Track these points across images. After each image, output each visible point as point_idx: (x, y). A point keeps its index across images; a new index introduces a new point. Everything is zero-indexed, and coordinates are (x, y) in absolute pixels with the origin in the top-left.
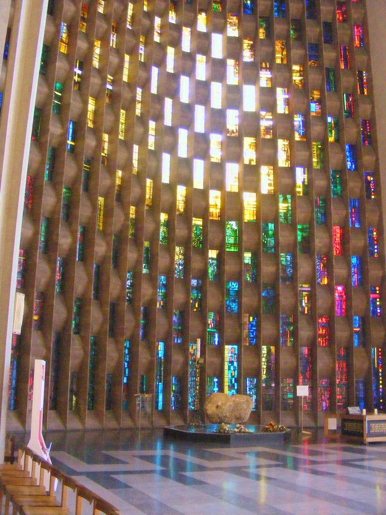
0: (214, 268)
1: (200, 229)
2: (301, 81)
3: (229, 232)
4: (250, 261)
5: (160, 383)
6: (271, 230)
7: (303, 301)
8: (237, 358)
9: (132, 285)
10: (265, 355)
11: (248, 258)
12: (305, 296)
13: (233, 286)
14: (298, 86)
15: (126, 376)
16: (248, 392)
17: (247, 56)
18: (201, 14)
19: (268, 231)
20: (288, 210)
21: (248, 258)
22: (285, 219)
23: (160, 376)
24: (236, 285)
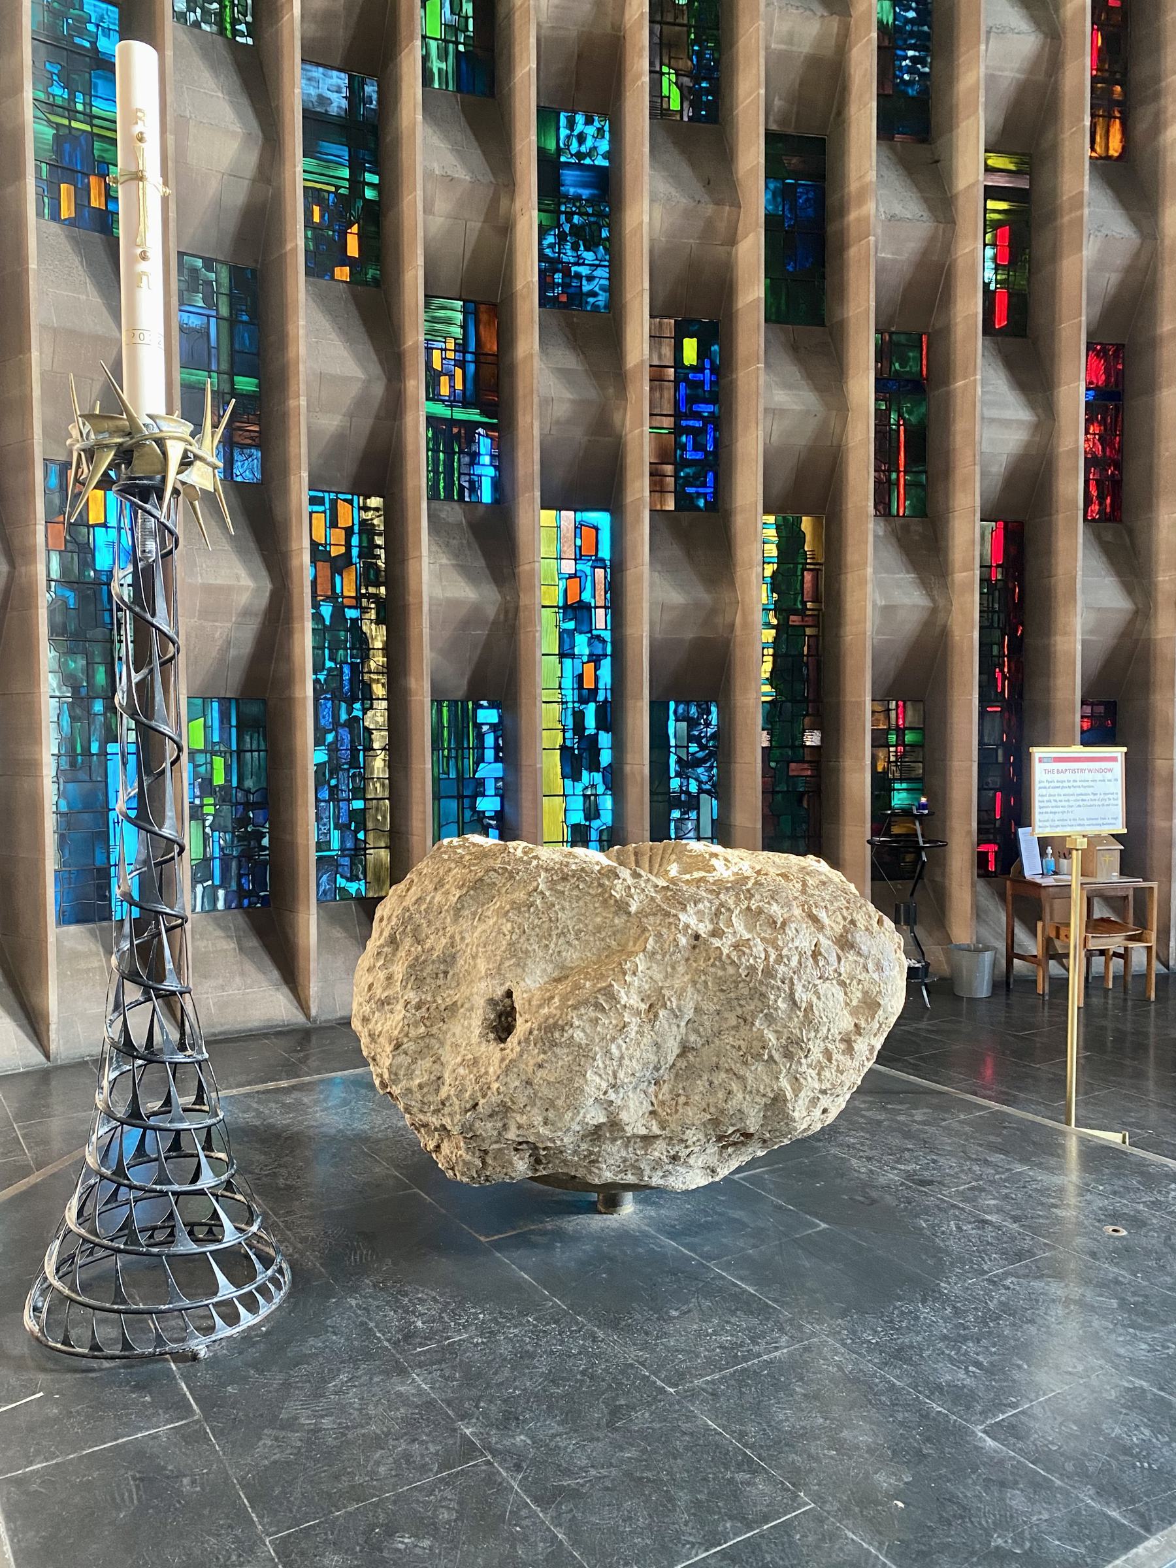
13: (581, 138)
16: (675, 783)
24: (600, 131)
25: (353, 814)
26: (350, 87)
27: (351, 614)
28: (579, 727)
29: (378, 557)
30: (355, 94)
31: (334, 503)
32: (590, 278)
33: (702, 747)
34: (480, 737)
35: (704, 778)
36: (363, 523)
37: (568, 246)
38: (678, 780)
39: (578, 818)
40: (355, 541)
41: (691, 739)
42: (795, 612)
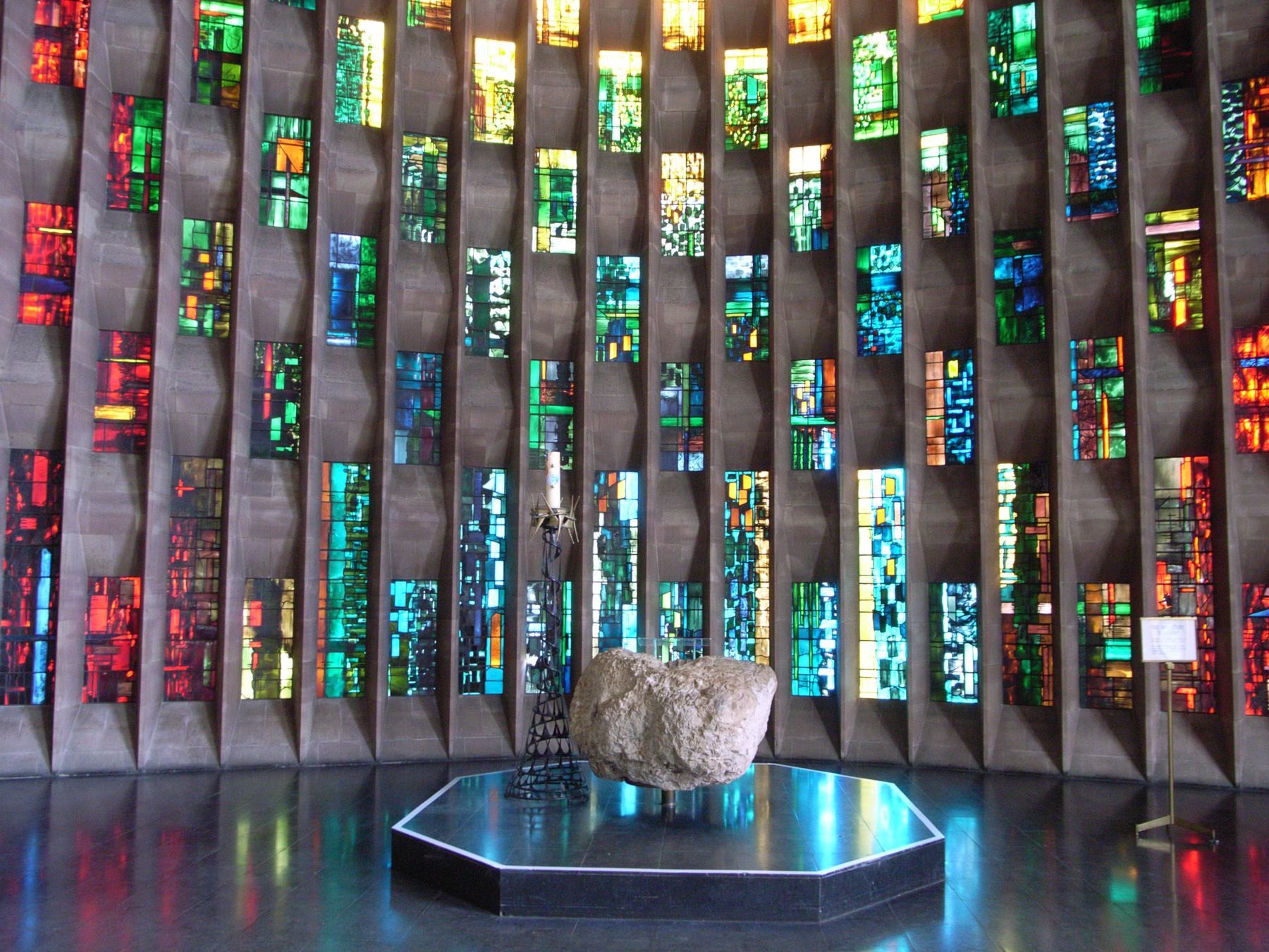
3: (863, 73)
4: (944, 159)
5: (625, 607)
6: (1025, 30)
7: (1168, 277)
8: (904, 513)
9: (514, 296)
10: (1010, 498)
12: (1174, 258)
13: (884, 259)
15: (496, 587)
19: (1012, 35)
23: (626, 583)
25: (748, 646)
26: (754, 262)
27: (749, 535)
28: (884, 600)
29: (765, 503)
30: (756, 266)
31: (741, 477)
32: (889, 335)
33: (966, 613)
34: (822, 604)
35: (968, 633)
36: (757, 486)
37: (877, 319)
38: (950, 634)
39: (885, 656)
40: (752, 496)
41: (958, 607)
42: (1029, 524)
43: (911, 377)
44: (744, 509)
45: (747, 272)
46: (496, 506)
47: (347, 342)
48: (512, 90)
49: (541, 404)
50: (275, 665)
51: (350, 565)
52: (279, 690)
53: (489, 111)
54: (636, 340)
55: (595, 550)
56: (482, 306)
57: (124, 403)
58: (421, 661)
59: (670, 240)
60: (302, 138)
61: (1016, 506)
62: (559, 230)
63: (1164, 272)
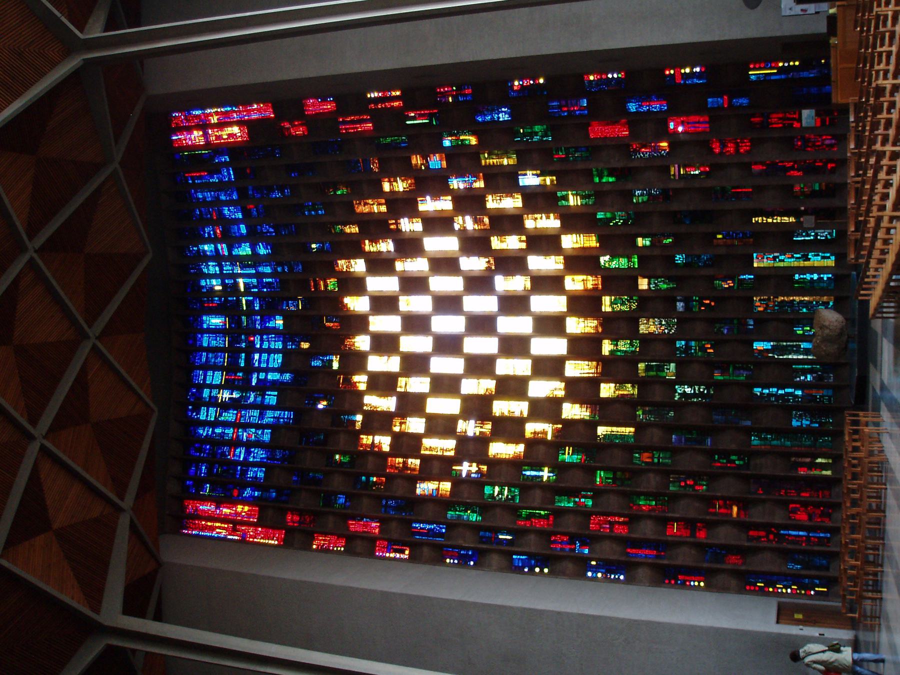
0: (660, 282)
1: (615, 300)
2: (403, 181)
3: (614, 264)
5: (802, 347)
7: (692, 173)
9: (690, 386)
10: (765, 219)
11: (644, 242)
12: (686, 171)
13: (680, 258)
14: (411, 184)
17: (386, 246)
18: (347, 304)
19: (607, 218)
20: (577, 195)
21: (644, 242)
22: (589, 199)
23: (793, 346)
27: (776, 303)
30: (680, 301)
43: (722, 251)
44: (767, 305)
45: (682, 304)
46: (766, 391)
47: (709, 440)
48: (618, 385)
49: (730, 376)
50: (821, 463)
51: (786, 440)
52: (829, 463)
53: (625, 393)
54: (706, 342)
55: (781, 357)
56: (694, 395)
57: (732, 509)
58: (820, 417)
59: (670, 331)
60: (640, 454)
61: (767, 217)
62: (667, 369)
63: (691, 174)
